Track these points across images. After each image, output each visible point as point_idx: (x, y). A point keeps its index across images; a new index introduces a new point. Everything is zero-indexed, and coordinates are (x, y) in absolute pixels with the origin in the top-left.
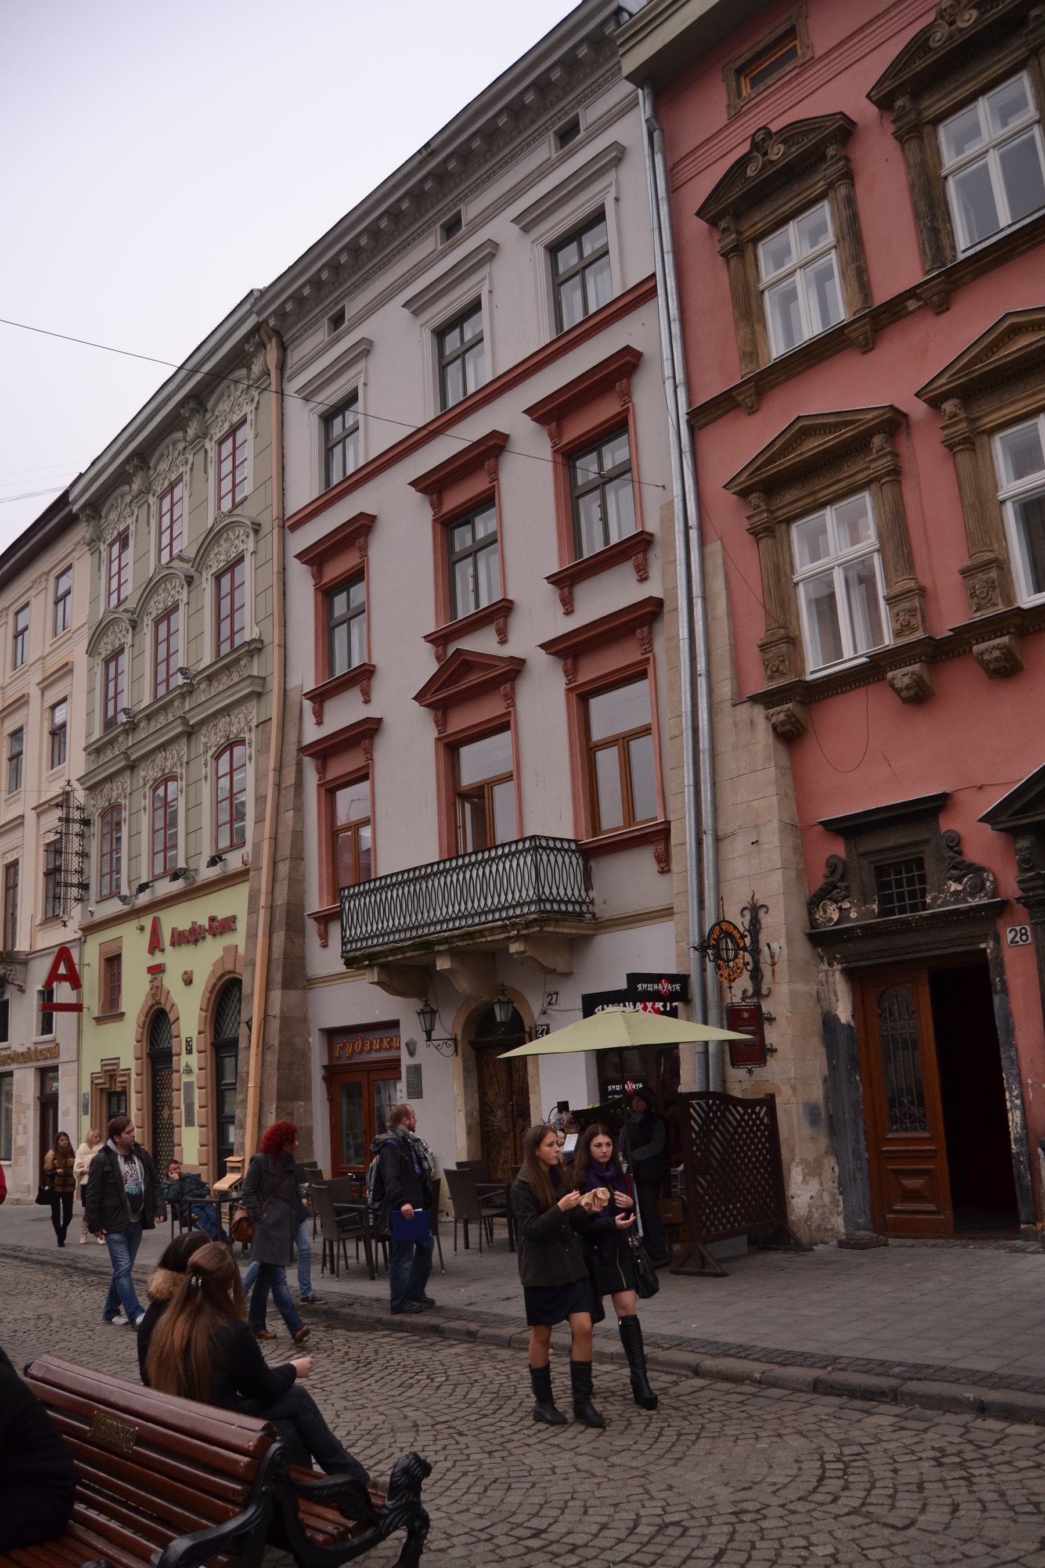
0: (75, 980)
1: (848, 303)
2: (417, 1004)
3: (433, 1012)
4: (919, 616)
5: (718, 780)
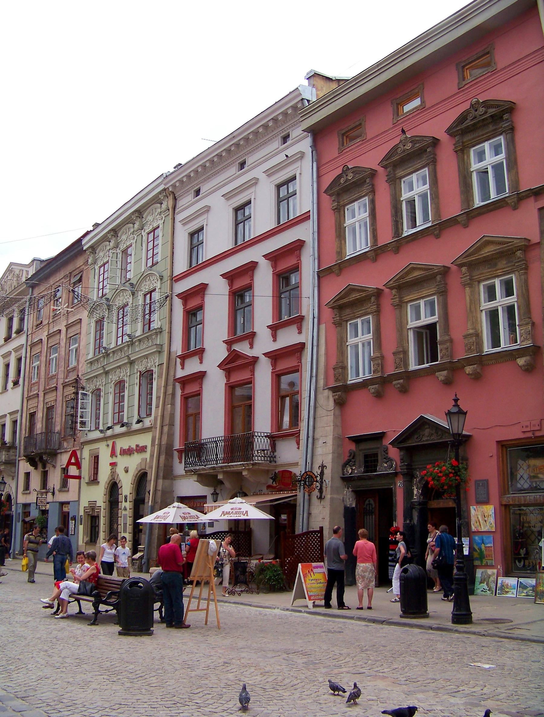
0: (78, 465)
2: (211, 490)
3: (217, 494)
5: (316, 417)
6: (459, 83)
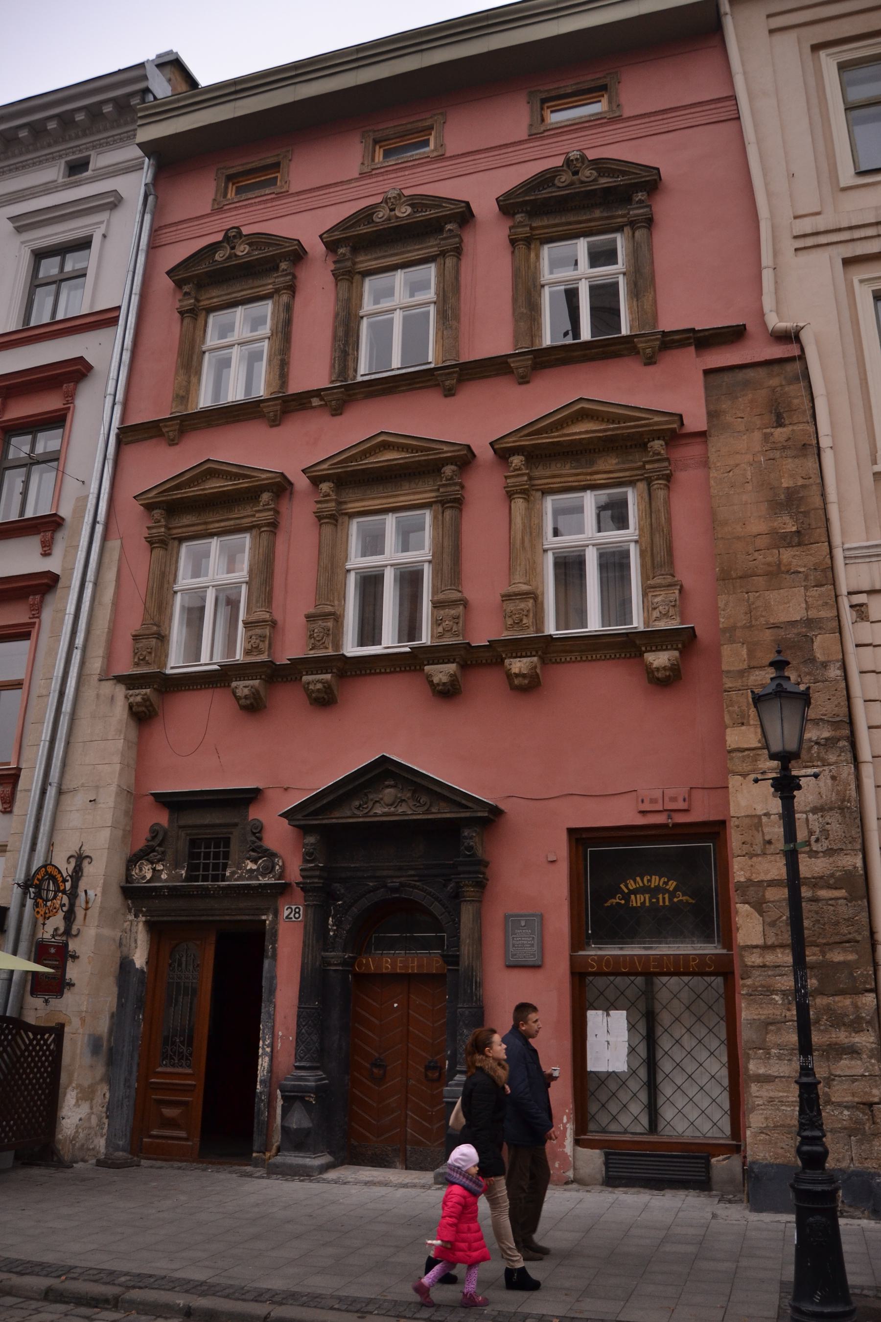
1: (268, 384)
4: (267, 642)
5: (72, 740)
6: (531, 125)
